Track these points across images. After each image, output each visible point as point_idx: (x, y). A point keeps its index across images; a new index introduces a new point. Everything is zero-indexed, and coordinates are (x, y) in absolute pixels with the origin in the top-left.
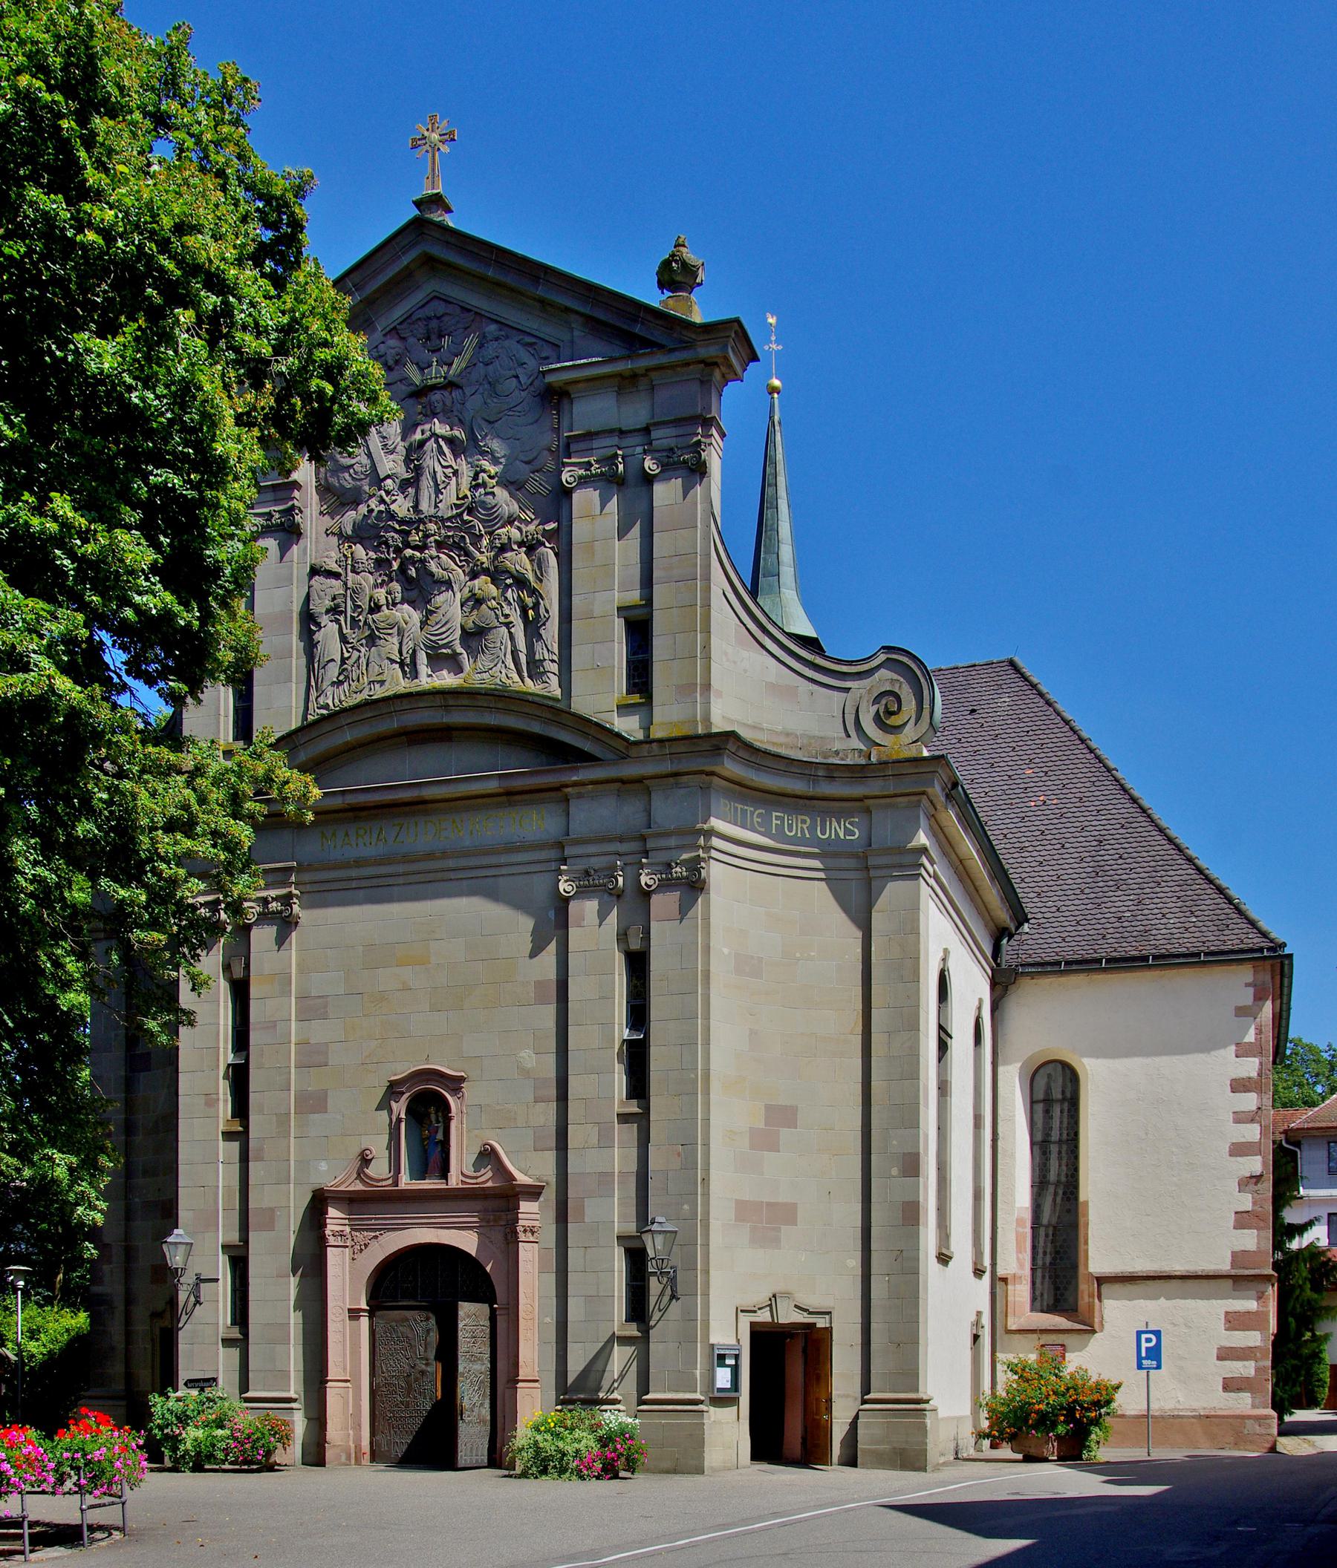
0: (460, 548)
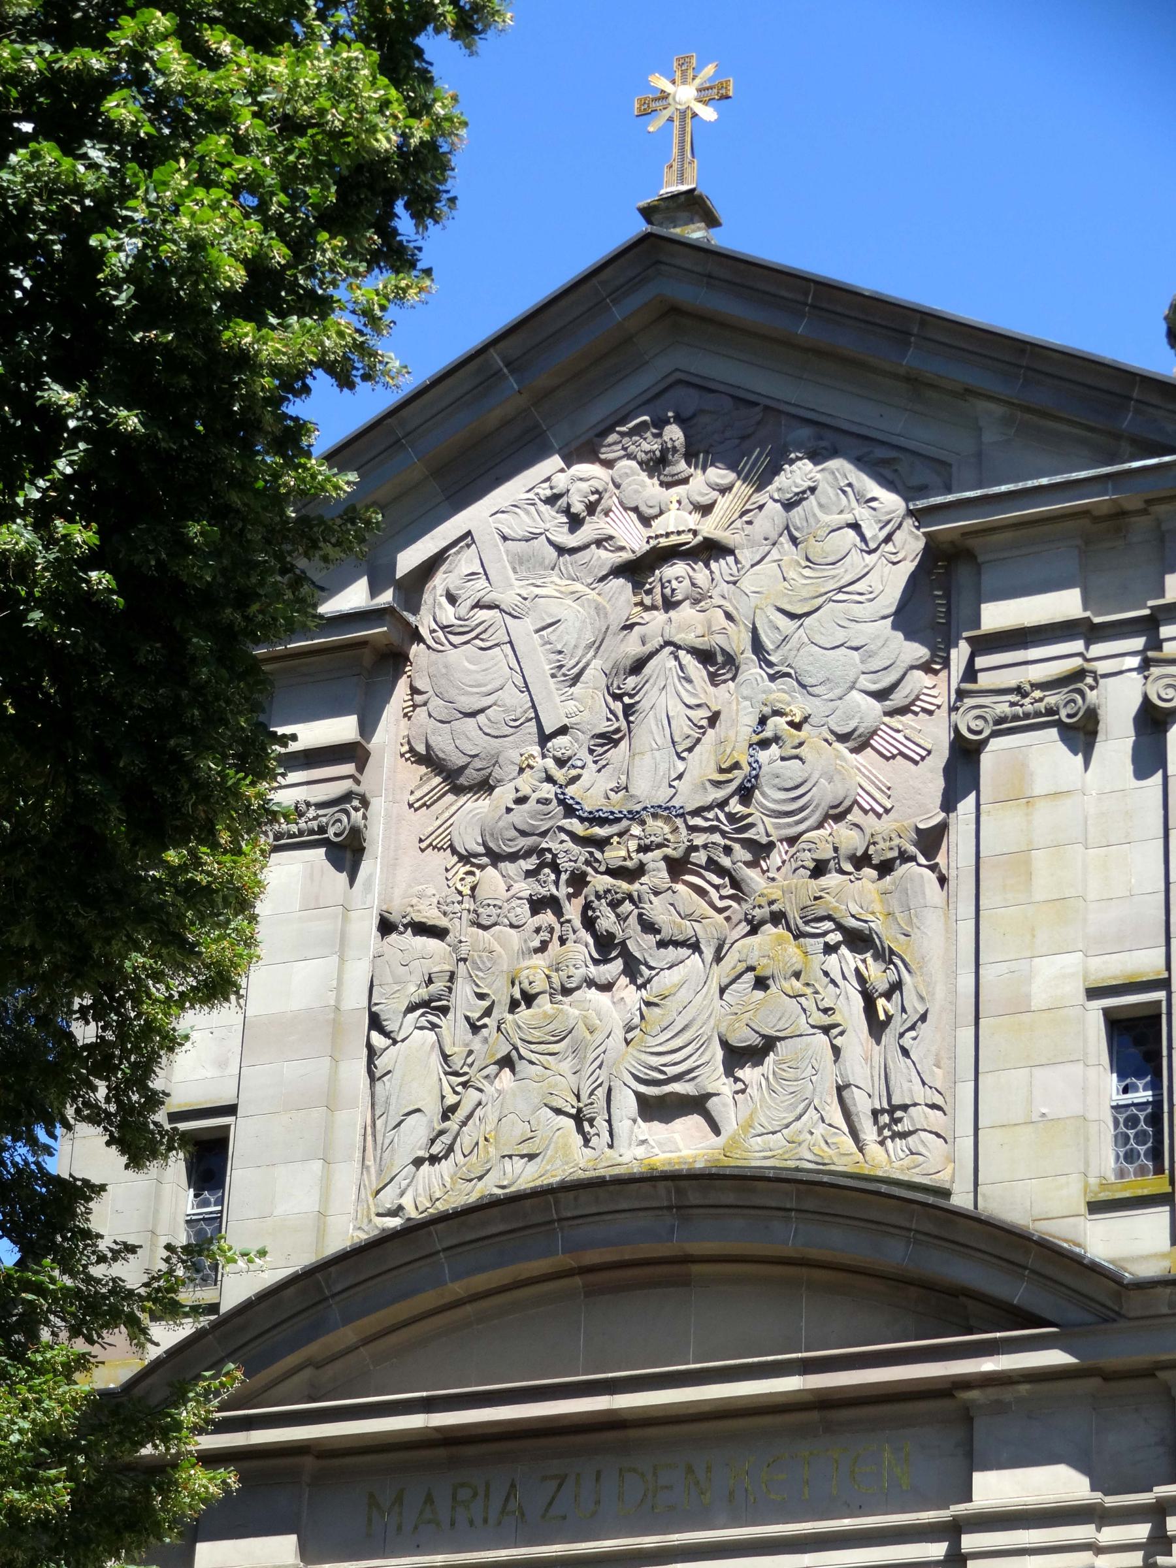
0: (722, 871)
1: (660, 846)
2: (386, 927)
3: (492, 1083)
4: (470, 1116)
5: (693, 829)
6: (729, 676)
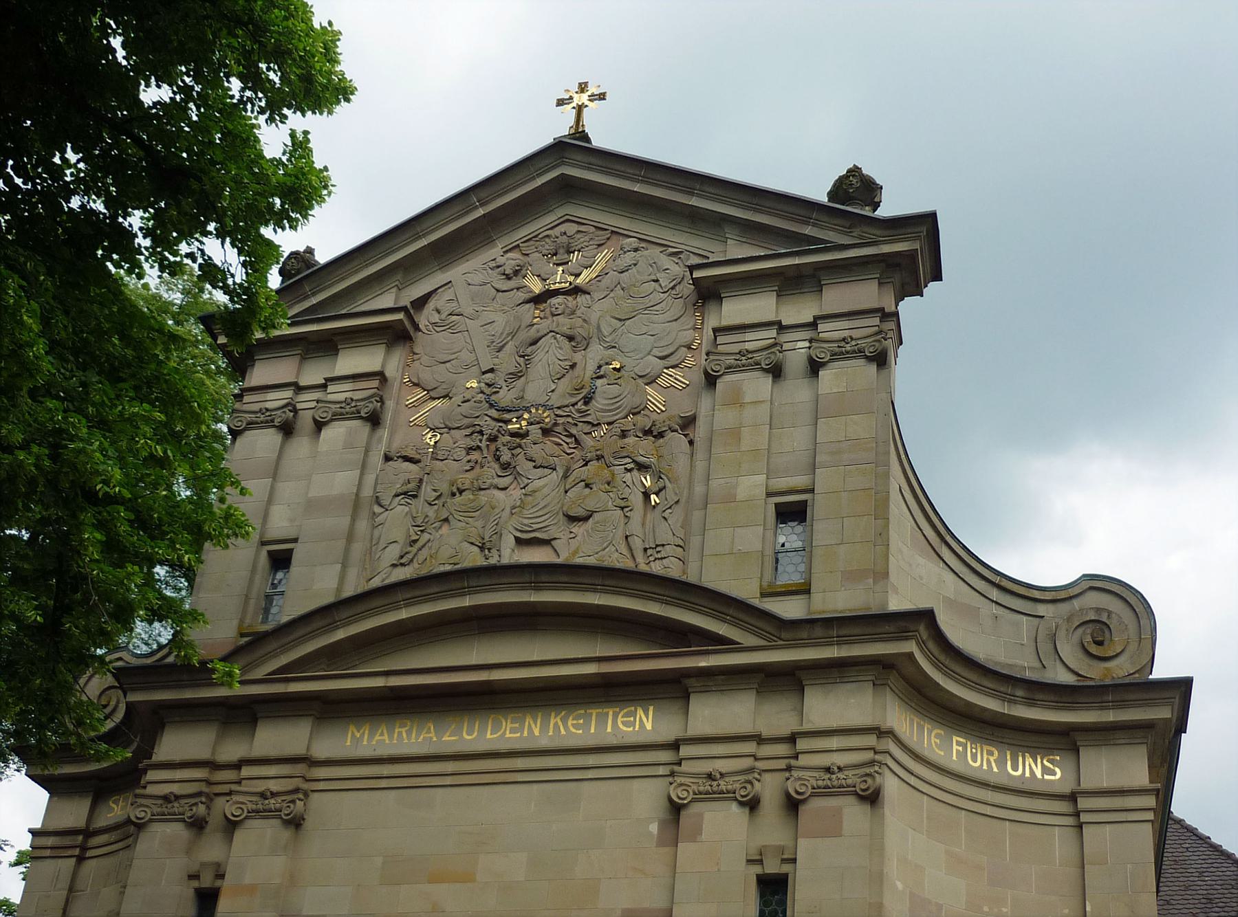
0: (571, 435)
1: (538, 423)
2: (387, 458)
3: (437, 531)
4: (423, 546)
5: (557, 416)
6: (583, 348)
